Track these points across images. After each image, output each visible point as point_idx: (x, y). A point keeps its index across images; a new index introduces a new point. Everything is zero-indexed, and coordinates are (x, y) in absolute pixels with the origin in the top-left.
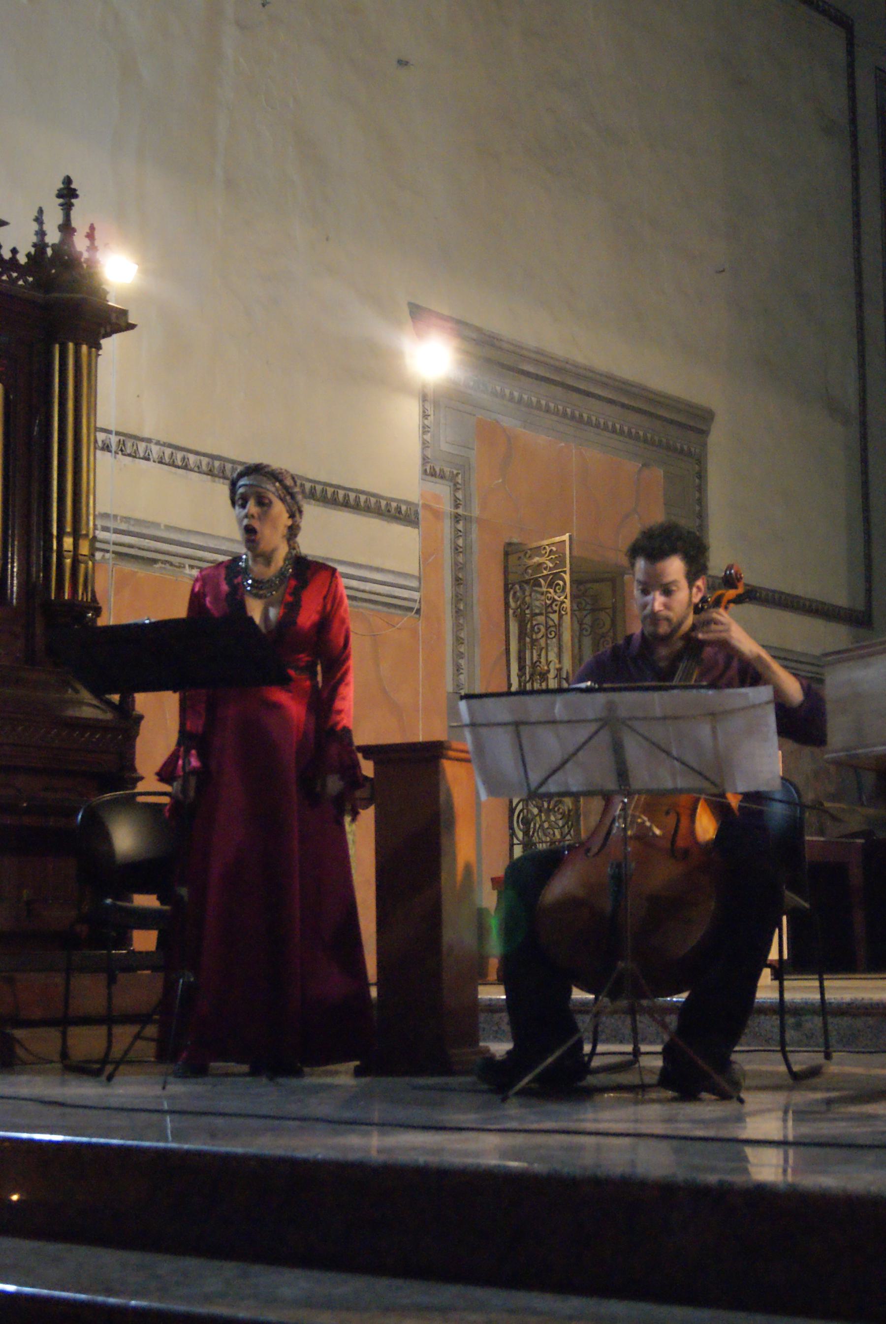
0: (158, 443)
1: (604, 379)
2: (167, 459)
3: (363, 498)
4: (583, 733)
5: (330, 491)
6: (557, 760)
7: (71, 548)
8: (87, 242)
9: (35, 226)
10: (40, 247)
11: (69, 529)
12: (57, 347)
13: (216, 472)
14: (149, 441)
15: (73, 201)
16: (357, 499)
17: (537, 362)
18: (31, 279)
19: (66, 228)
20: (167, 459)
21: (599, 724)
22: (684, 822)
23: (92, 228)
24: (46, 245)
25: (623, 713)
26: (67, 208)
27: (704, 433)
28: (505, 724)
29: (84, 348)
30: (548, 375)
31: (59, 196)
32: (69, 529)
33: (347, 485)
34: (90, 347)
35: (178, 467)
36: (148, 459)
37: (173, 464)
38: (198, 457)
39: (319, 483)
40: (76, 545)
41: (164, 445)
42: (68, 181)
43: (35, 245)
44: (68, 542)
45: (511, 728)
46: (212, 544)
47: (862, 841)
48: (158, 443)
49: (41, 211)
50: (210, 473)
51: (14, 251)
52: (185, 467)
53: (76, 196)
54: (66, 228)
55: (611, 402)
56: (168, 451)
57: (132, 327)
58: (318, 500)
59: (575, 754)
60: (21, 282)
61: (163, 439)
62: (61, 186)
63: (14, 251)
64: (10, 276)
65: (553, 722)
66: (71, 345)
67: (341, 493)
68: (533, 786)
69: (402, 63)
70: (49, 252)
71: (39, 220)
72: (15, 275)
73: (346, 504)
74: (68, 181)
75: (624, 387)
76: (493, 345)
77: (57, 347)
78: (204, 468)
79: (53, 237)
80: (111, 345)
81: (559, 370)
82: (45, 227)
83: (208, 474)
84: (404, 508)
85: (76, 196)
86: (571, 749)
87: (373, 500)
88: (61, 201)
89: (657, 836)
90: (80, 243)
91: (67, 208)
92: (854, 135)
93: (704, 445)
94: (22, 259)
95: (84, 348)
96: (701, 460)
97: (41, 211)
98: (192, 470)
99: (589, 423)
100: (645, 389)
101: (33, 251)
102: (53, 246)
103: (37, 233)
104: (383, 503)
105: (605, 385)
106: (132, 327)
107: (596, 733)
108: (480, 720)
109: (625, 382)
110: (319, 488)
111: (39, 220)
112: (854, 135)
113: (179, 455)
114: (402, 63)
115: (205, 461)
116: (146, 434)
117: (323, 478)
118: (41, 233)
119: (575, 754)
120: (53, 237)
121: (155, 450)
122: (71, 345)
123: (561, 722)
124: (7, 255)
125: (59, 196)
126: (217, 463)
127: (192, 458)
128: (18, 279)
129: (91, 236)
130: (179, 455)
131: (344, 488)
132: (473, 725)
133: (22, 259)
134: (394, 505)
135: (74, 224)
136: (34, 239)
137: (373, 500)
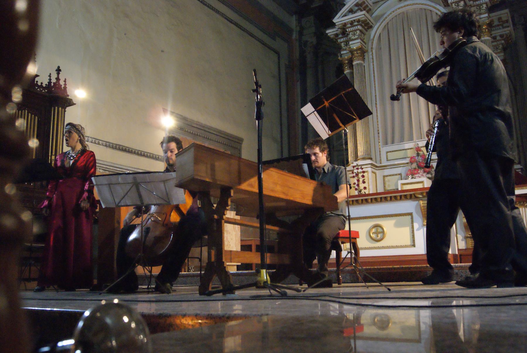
0: (91, 138)
1: (209, 127)
2: (93, 142)
3: (149, 154)
4: (128, 187)
5: (140, 152)
6: (123, 195)
7: (54, 159)
8: (64, 83)
9: (49, 78)
10: (50, 83)
11: (54, 154)
12: (53, 108)
13: (107, 146)
14: (88, 137)
15: (60, 72)
16: (150, 155)
17: (197, 124)
18: (46, 91)
19: (58, 79)
20: (93, 142)
21: (133, 184)
22: (168, 215)
23: (65, 79)
24: (51, 82)
25: (139, 181)
26: (58, 74)
27: (241, 144)
28: (106, 184)
29: (60, 109)
30: (200, 128)
31: (56, 71)
32: (54, 154)
33: (144, 151)
34: (62, 109)
35: (97, 144)
36: (88, 141)
37: (95, 143)
38: (103, 142)
39: (136, 150)
40: (55, 158)
41: (93, 138)
42: (59, 67)
43: (48, 82)
44: (53, 157)
45: (108, 186)
46: (106, 163)
47: (277, 240)
48: (91, 138)
49: (50, 74)
50: (106, 146)
51: (42, 83)
52: (99, 144)
53: (61, 71)
54: (58, 79)
55: (217, 135)
56: (94, 140)
57: (75, 104)
58: (136, 154)
59: (127, 194)
60: (43, 91)
61: (92, 137)
62: (57, 68)
63: (42, 83)
64: (40, 89)
65: (119, 184)
66: (56, 108)
67: (143, 153)
68: (117, 203)
69: (162, 51)
70: (52, 84)
71: (50, 76)
72: (41, 89)
73: (144, 156)
74: (59, 67)
75: (220, 132)
76: (185, 120)
77: (53, 108)
78: (104, 144)
79: (54, 80)
80: (68, 109)
81: (204, 127)
82: (51, 78)
83: (105, 146)
84: (160, 157)
85: (61, 71)
86: (126, 192)
87: (151, 155)
88: (57, 72)
89: (160, 220)
90: (62, 83)
91: (58, 74)
92: (280, 78)
93: (241, 147)
94: (44, 86)
95: (60, 109)
96: (240, 150)
97: (50, 74)
98: (100, 145)
99: (211, 140)
100: (225, 132)
101: (47, 84)
102: (54, 83)
103: (49, 79)
104: (154, 156)
105: (214, 131)
106: (75, 104)
107: (132, 187)
108: (99, 183)
109: (221, 131)
110: (136, 151)
111: (50, 76)
112: (280, 78)
113: (97, 141)
114: (162, 51)
115: (104, 143)
116: (88, 136)
117: (138, 149)
118: (50, 80)
119: (127, 194)
120: (54, 80)
121: (90, 139)
122: (56, 108)
123: (122, 184)
124: (39, 84)
125: (56, 71)
126: (108, 144)
127: (101, 142)
128: (42, 90)
129: (65, 81)
130: (97, 141)
131: (144, 152)
132: (97, 185)
133: (44, 86)
134: (157, 156)
135: (60, 78)
136: (48, 81)
137: (151, 155)
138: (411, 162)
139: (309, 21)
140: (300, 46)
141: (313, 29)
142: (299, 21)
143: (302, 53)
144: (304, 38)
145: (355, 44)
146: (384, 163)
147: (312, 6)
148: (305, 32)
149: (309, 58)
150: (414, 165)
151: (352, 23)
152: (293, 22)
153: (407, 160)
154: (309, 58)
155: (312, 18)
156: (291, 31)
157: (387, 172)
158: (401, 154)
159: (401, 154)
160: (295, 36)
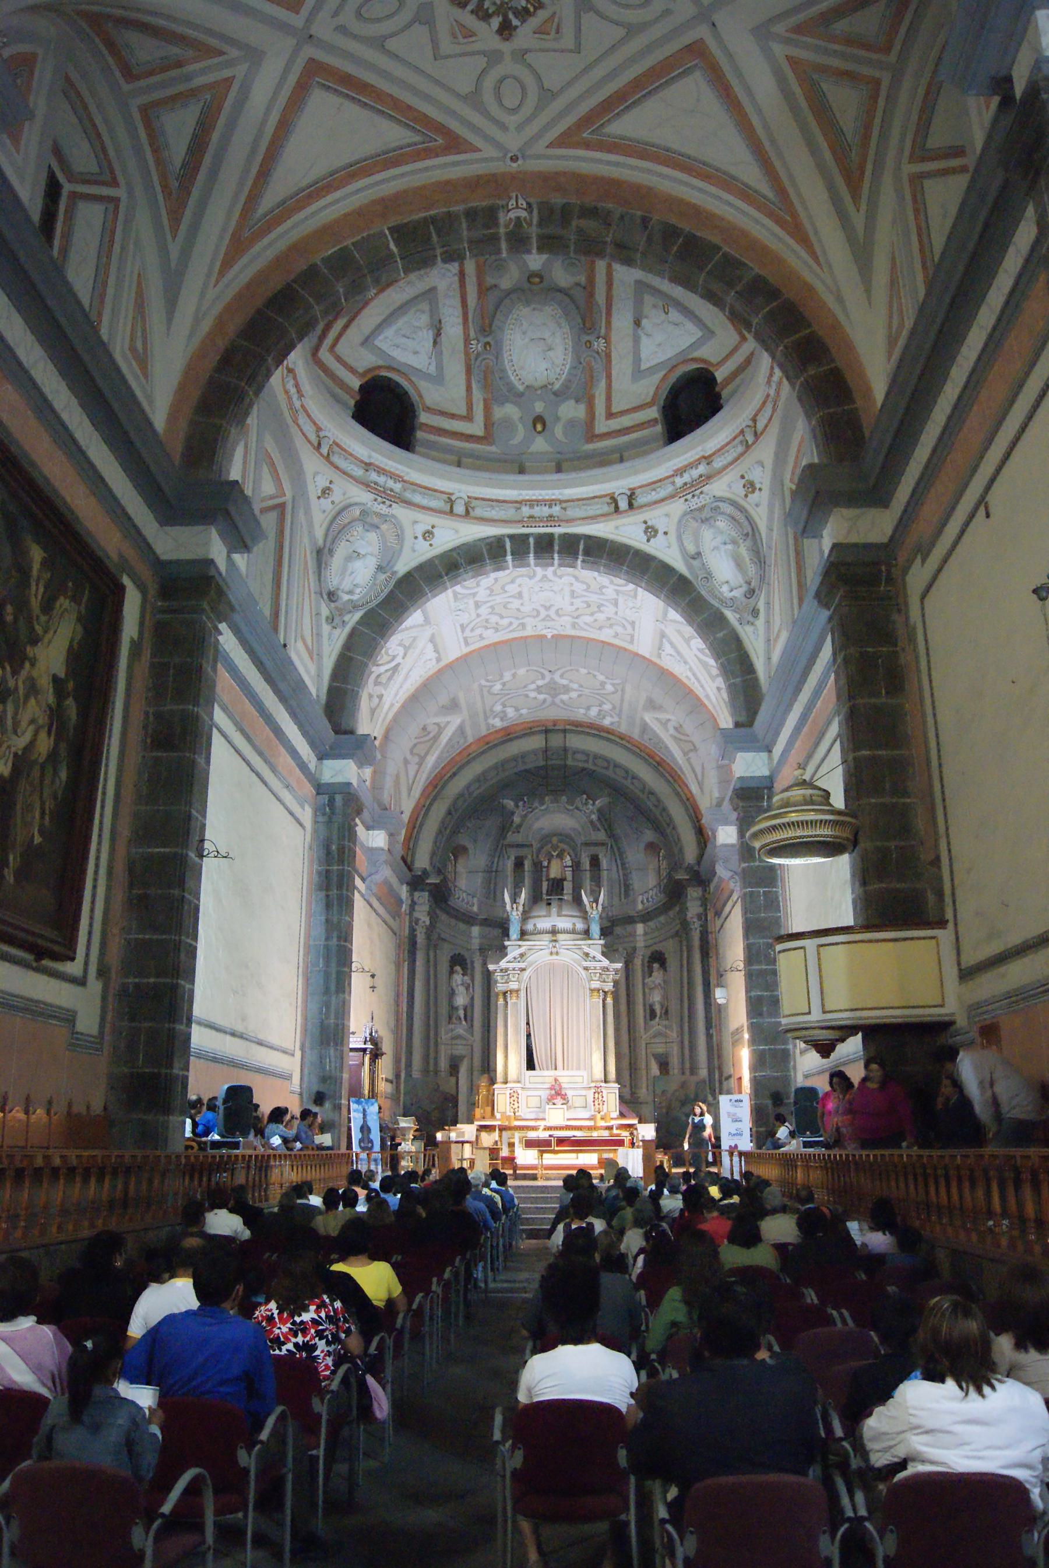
138: (551, 1089)
139: (423, 898)
140: (410, 922)
141: (426, 908)
142: (412, 895)
143: (412, 930)
144: (416, 915)
145: (513, 986)
146: (528, 1085)
147: (428, 881)
148: (416, 907)
149: (421, 939)
150: (553, 1092)
151: (514, 969)
152: (404, 891)
153: (548, 1086)
154: (421, 939)
155: (427, 894)
156: (400, 902)
157: (530, 1093)
158: (540, 1080)
159: (540, 1080)
160: (404, 907)
